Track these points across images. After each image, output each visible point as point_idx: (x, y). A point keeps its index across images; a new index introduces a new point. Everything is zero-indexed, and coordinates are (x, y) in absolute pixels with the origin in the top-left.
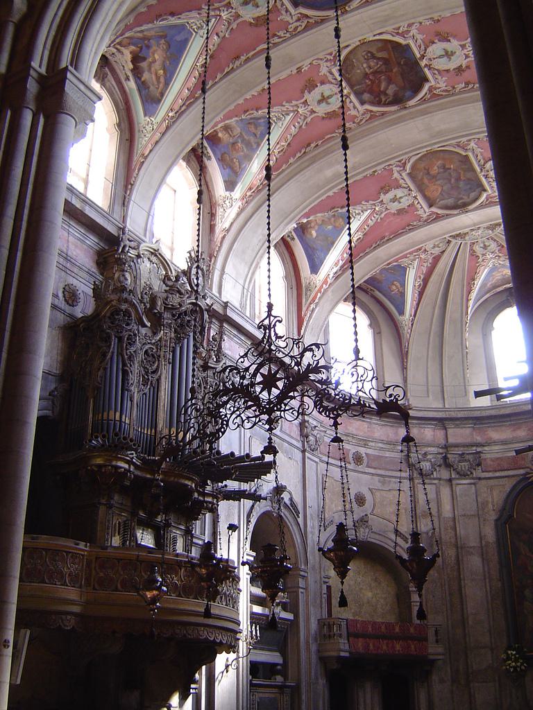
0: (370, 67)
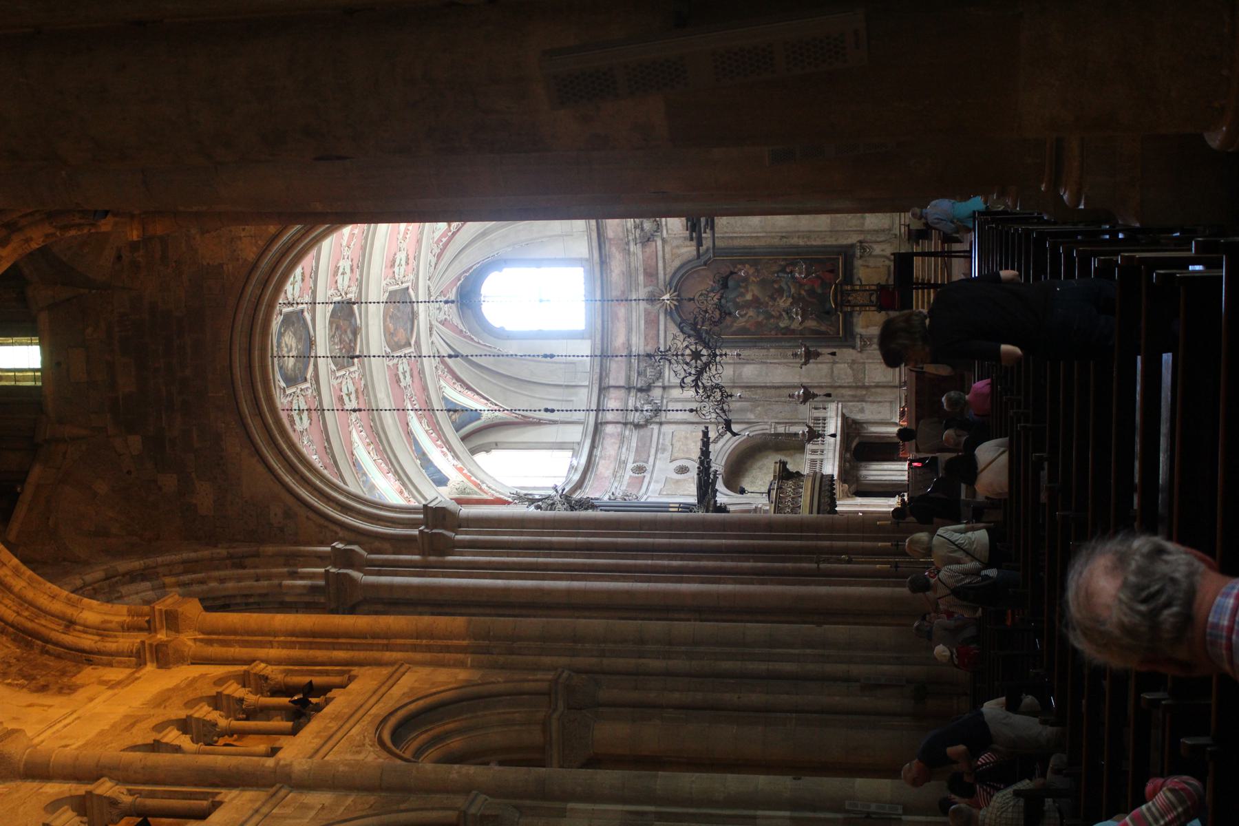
0: (337, 344)
